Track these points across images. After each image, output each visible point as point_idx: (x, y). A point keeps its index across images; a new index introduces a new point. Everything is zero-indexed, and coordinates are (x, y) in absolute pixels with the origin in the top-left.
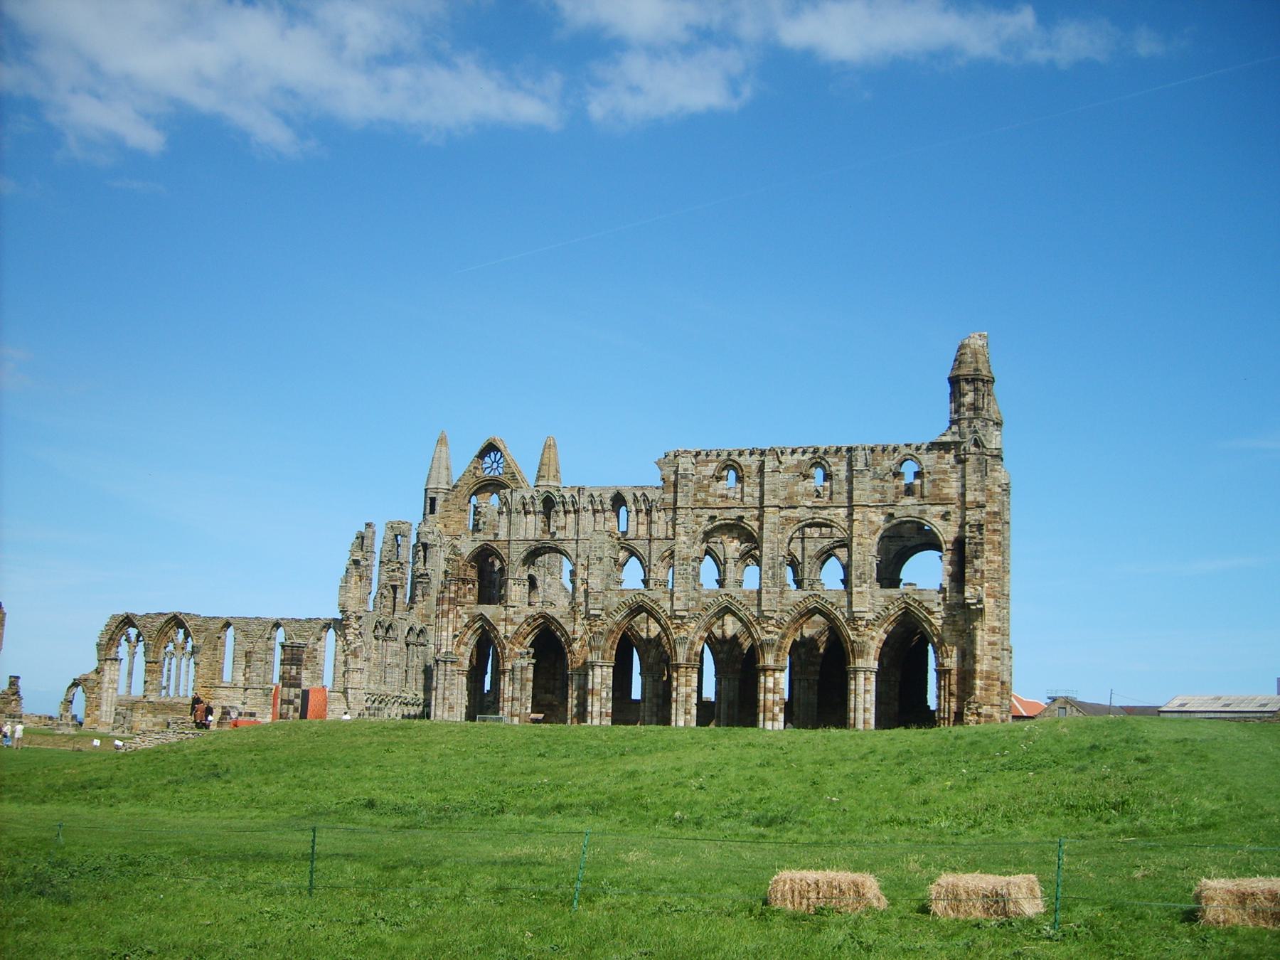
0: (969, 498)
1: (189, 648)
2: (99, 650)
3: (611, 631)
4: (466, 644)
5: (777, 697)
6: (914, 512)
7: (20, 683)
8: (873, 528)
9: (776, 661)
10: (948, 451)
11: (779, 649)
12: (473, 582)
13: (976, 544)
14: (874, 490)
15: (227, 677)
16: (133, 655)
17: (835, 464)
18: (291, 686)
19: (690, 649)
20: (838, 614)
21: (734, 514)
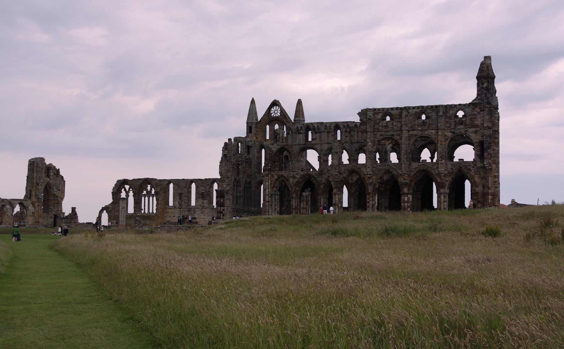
0: (485, 125)
1: (153, 192)
2: (113, 195)
3: (342, 181)
4: (276, 187)
5: (409, 204)
6: (463, 131)
7: (76, 210)
8: (446, 138)
9: (408, 191)
10: (476, 107)
11: (410, 186)
12: (277, 162)
13: (489, 143)
14: (446, 122)
15: (171, 203)
16: (127, 196)
17: (430, 113)
18: (220, 207)
19: (374, 187)
20: (433, 171)
21: (391, 133)
